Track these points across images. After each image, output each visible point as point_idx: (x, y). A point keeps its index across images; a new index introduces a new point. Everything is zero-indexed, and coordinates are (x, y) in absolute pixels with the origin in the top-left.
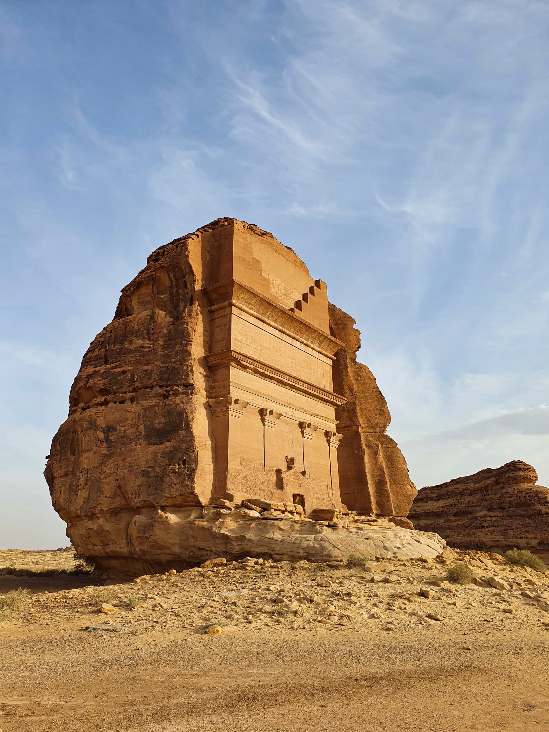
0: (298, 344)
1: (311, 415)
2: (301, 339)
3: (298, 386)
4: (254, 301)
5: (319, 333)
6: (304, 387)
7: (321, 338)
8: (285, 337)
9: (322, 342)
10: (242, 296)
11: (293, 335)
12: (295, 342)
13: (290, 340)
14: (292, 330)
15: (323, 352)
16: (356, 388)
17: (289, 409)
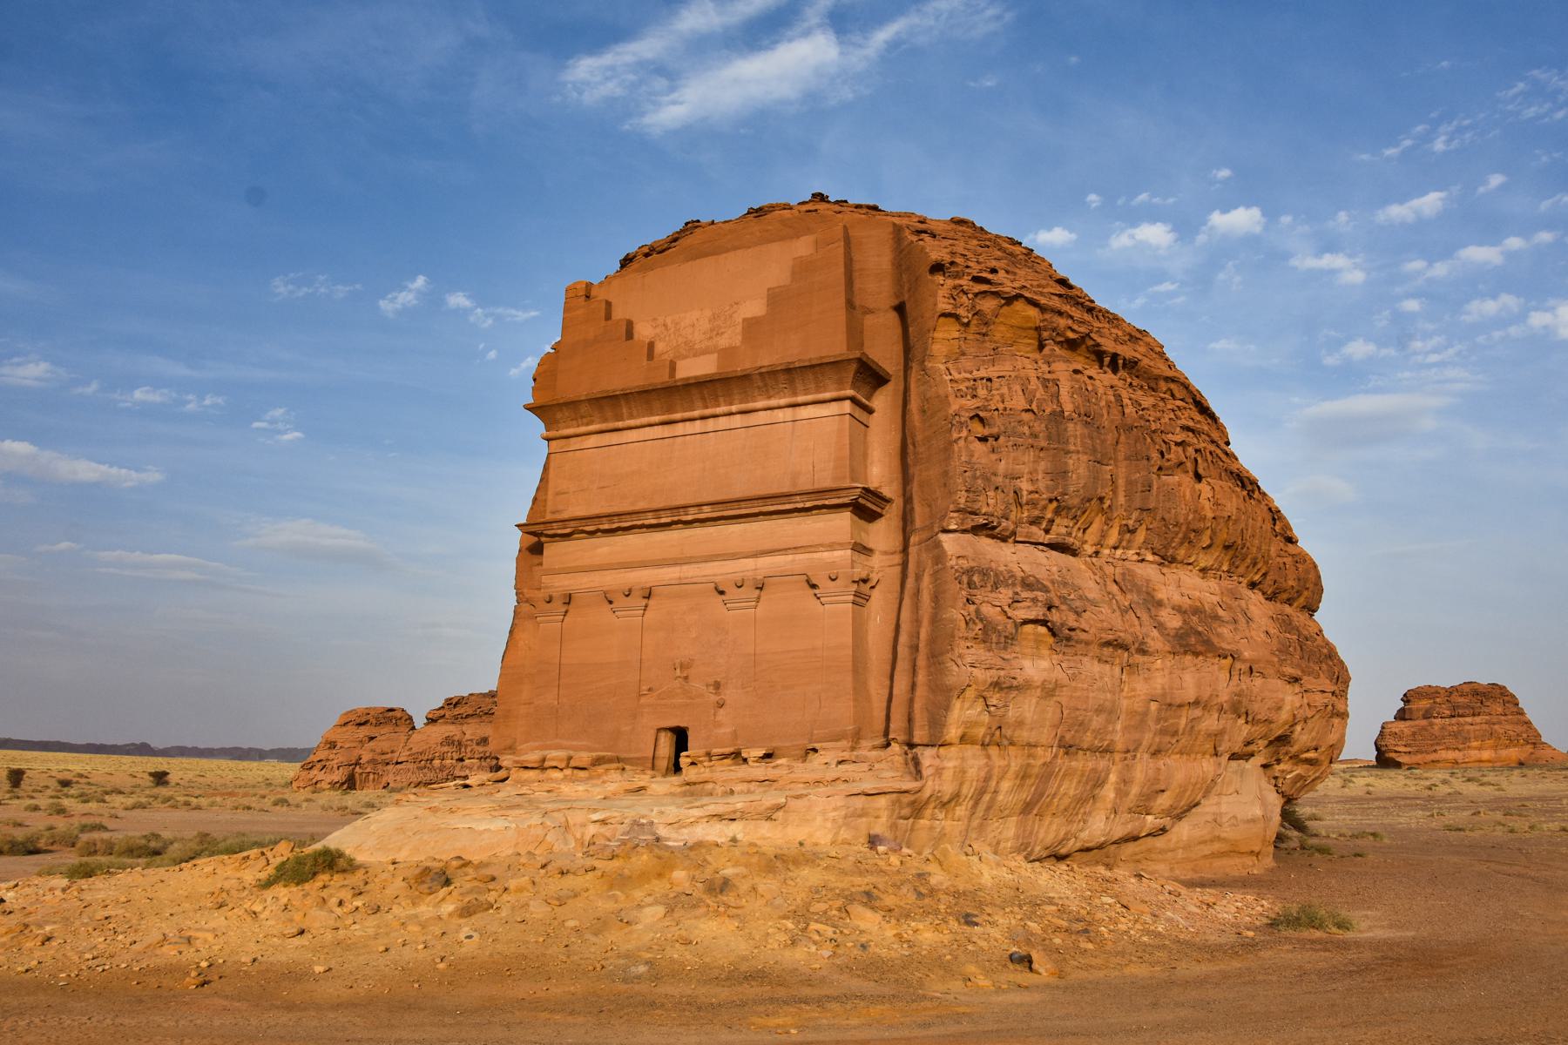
0: (723, 422)
1: (755, 555)
2: (719, 410)
3: (689, 518)
4: (584, 409)
5: (761, 374)
6: (707, 512)
7: (782, 377)
8: (680, 429)
9: (791, 382)
10: (559, 415)
11: (696, 413)
12: (711, 424)
13: (698, 426)
14: (700, 403)
15: (800, 399)
16: (919, 438)
17: (685, 567)
